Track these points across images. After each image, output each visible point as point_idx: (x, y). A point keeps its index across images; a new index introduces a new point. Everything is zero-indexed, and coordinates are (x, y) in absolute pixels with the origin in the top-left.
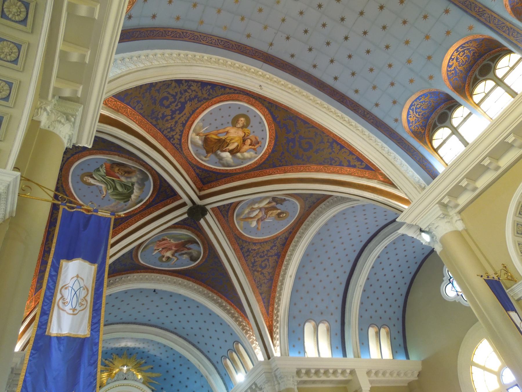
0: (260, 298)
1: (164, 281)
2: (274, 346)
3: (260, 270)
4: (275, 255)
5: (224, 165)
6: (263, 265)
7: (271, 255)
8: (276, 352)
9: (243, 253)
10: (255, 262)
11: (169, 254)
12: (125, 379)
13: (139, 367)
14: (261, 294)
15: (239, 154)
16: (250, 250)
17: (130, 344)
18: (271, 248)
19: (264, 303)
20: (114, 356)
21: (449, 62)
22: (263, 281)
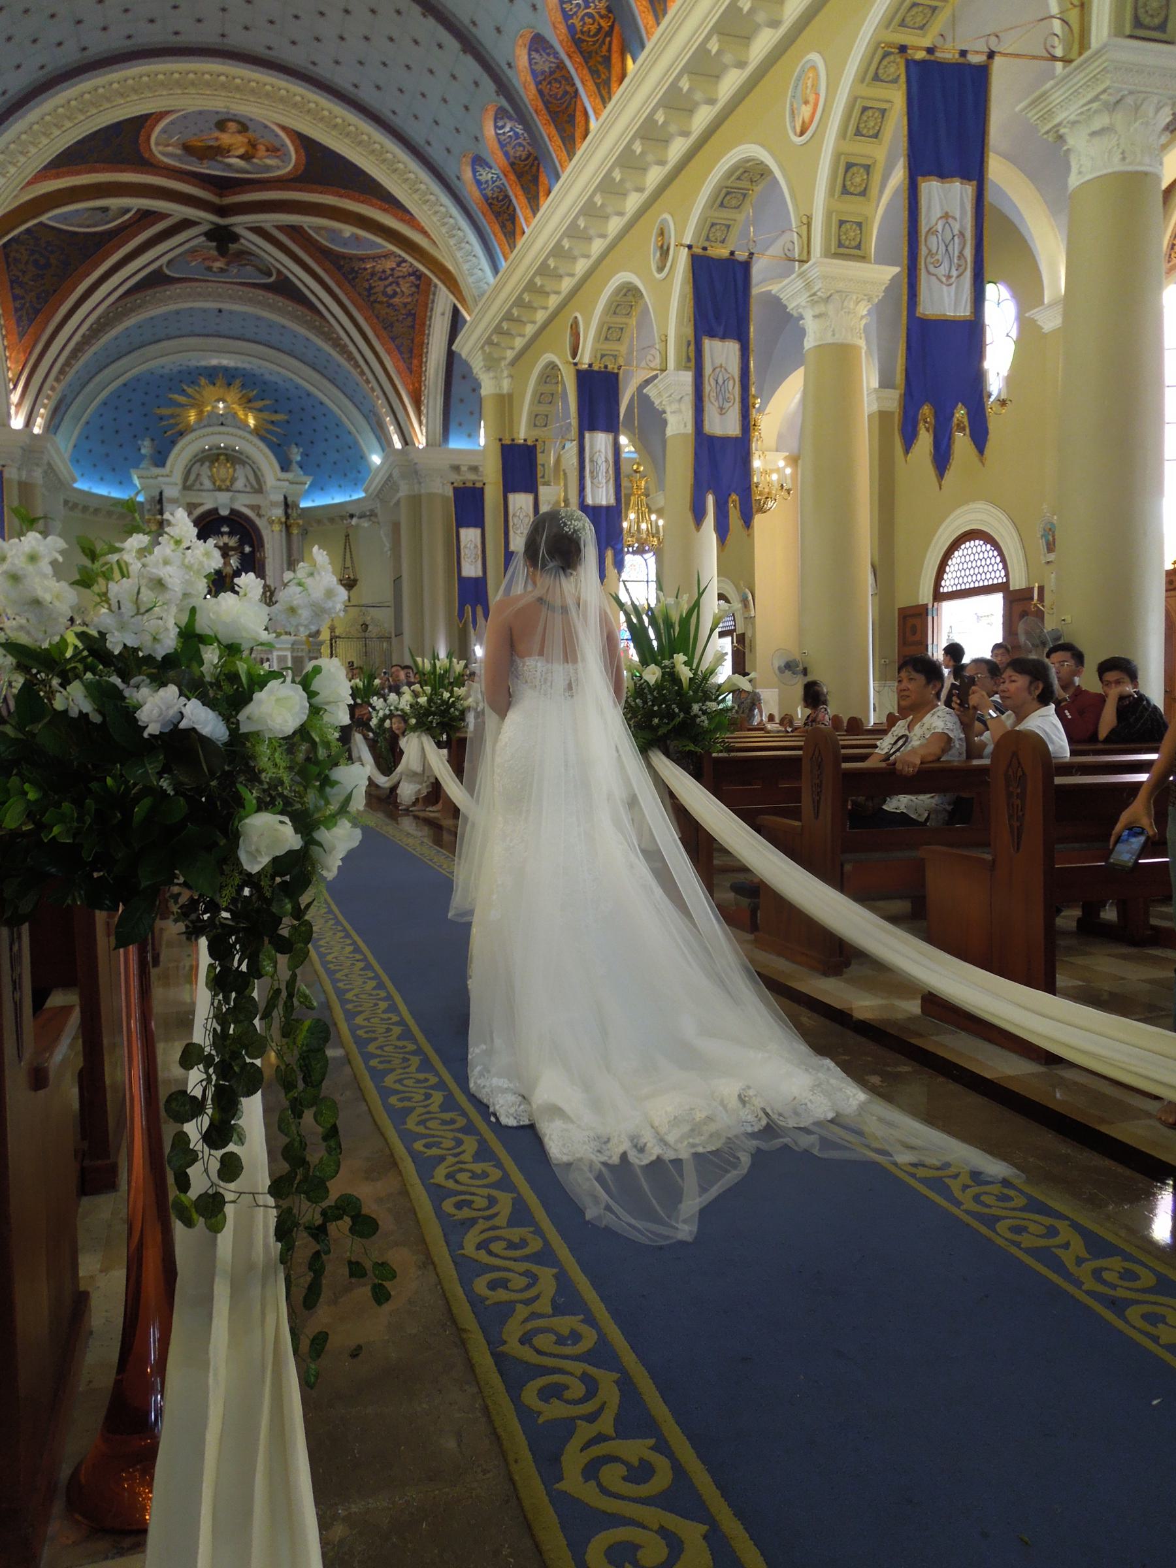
0: (392, 345)
1: (230, 297)
2: (420, 423)
3: (385, 300)
4: (410, 275)
5: (238, 171)
6: (389, 290)
7: (401, 274)
8: (421, 441)
9: (343, 274)
10: (371, 288)
11: (218, 265)
12: (222, 424)
13: (248, 403)
14: (393, 339)
15: (255, 160)
16: (356, 269)
17: (225, 362)
18: (399, 265)
19: (401, 353)
20: (203, 381)
21: (495, 122)
22: (395, 318)
